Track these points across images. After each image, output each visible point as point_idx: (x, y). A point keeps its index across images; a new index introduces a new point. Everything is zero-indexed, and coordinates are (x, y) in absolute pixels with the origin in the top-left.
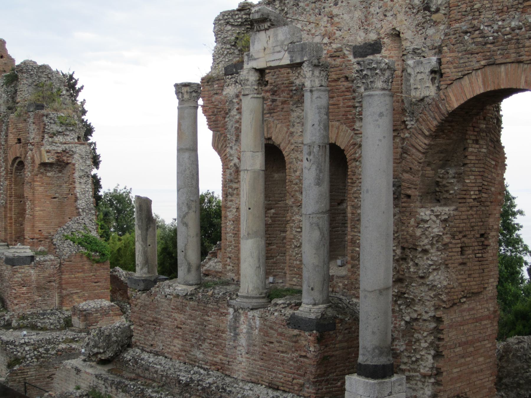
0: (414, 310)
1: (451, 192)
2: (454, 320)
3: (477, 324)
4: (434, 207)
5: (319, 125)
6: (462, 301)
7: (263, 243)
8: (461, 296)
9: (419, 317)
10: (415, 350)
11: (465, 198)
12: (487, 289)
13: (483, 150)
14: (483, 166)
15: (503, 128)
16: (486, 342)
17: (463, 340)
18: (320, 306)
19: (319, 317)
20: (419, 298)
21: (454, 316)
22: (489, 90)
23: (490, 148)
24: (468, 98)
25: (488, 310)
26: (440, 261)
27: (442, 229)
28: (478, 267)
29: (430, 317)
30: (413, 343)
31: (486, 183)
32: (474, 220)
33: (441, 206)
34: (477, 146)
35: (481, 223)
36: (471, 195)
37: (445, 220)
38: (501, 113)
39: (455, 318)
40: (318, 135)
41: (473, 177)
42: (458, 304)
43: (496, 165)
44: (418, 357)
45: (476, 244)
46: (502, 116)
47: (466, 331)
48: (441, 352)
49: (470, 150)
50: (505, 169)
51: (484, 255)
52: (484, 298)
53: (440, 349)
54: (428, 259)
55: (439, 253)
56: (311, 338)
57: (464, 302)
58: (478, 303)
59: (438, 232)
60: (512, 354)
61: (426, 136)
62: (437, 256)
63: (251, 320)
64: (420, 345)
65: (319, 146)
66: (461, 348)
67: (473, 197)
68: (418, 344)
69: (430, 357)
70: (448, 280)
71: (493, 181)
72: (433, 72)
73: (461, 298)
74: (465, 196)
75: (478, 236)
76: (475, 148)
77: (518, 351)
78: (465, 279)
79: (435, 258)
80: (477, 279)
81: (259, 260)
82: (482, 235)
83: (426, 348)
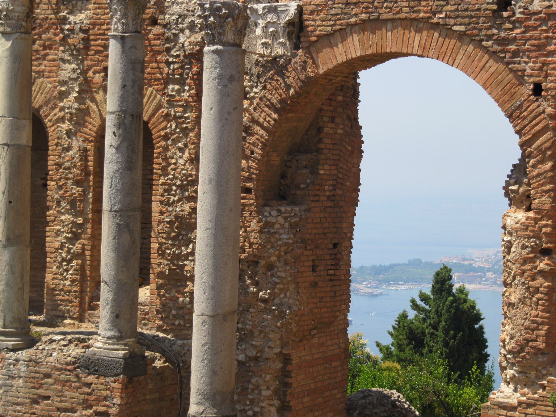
0: (252, 345)
1: (302, 186)
2: (303, 358)
3: (327, 365)
4: (281, 205)
5: (133, 87)
6: (313, 333)
7: (28, 254)
8: (310, 327)
9: (259, 355)
10: (252, 401)
11: (318, 195)
12: (339, 318)
13: (340, 131)
14: (338, 152)
15: (360, 101)
16: (336, 391)
17: (312, 386)
18: (128, 340)
19: (127, 356)
20: (259, 328)
21: (304, 354)
22: (369, 52)
23: (346, 128)
24: (340, 61)
25: (339, 347)
26: (289, 279)
27: (292, 236)
28: (329, 289)
29: (275, 354)
30: (249, 390)
31: (341, 176)
32: (327, 225)
33: (288, 204)
34: (333, 125)
35: (334, 230)
36: (325, 191)
37: (296, 225)
38: (358, 81)
39: (304, 356)
40: (131, 100)
41: (327, 167)
42: (308, 337)
43: (352, 152)
44: (257, 409)
45: (328, 257)
46: (360, 84)
47: (315, 375)
48: (289, 401)
49: (326, 130)
50: (361, 157)
51: (337, 273)
52: (334, 330)
53: (288, 397)
54: (272, 275)
55: (288, 268)
56: (117, 385)
57: (315, 335)
58: (328, 338)
59: (287, 239)
60: (357, 412)
61: (276, 110)
62: (285, 271)
63: (12, 366)
64: (260, 393)
65: (132, 115)
66: (310, 397)
67: (327, 193)
68: (256, 392)
69: (273, 409)
70: (298, 303)
71: (348, 174)
72: (290, 23)
73: (311, 329)
74: (318, 192)
75: (331, 246)
76: (331, 128)
77: (365, 408)
78: (316, 304)
79: (283, 275)
80: (329, 305)
81: (22, 277)
82: (335, 245)
83: (269, 398)
